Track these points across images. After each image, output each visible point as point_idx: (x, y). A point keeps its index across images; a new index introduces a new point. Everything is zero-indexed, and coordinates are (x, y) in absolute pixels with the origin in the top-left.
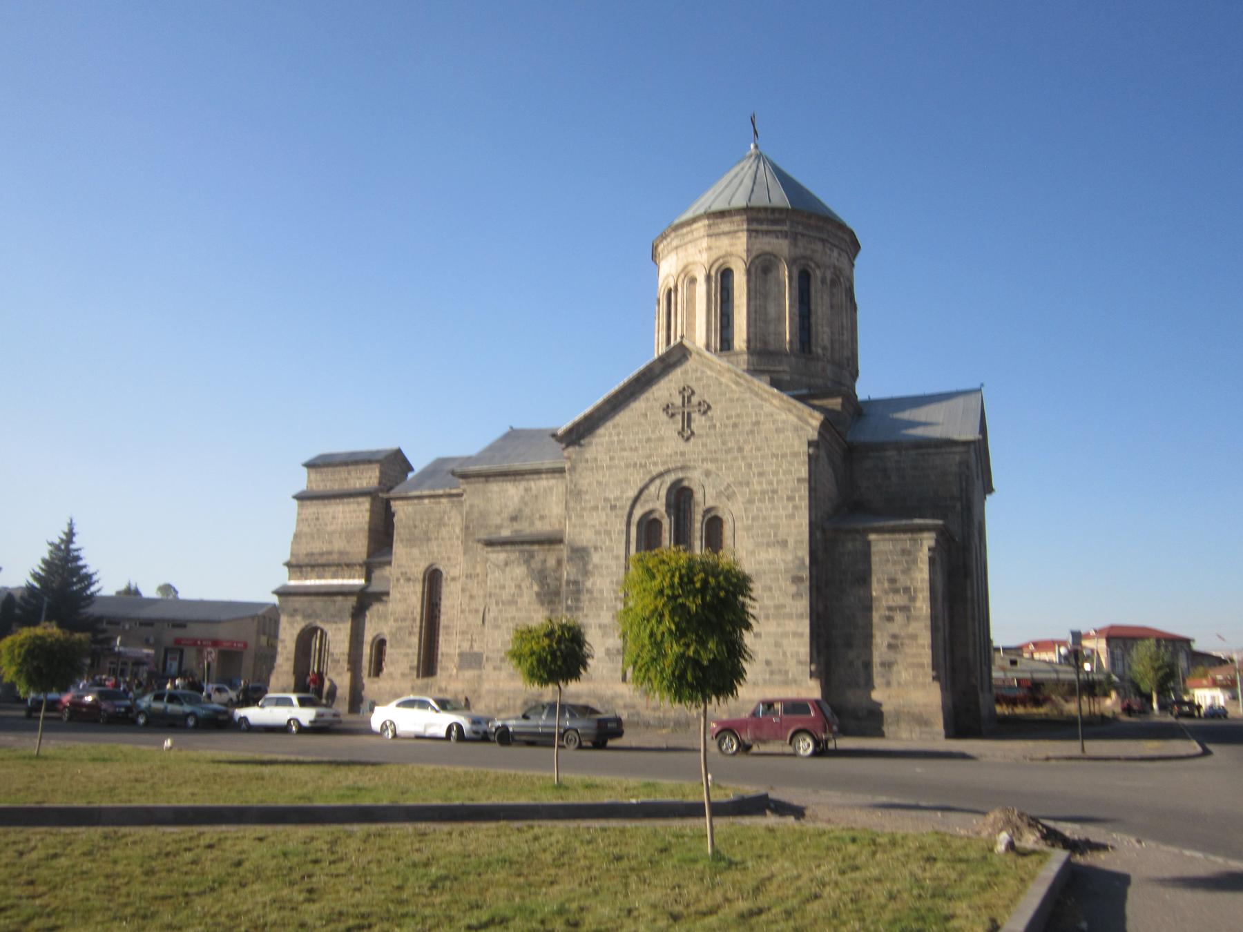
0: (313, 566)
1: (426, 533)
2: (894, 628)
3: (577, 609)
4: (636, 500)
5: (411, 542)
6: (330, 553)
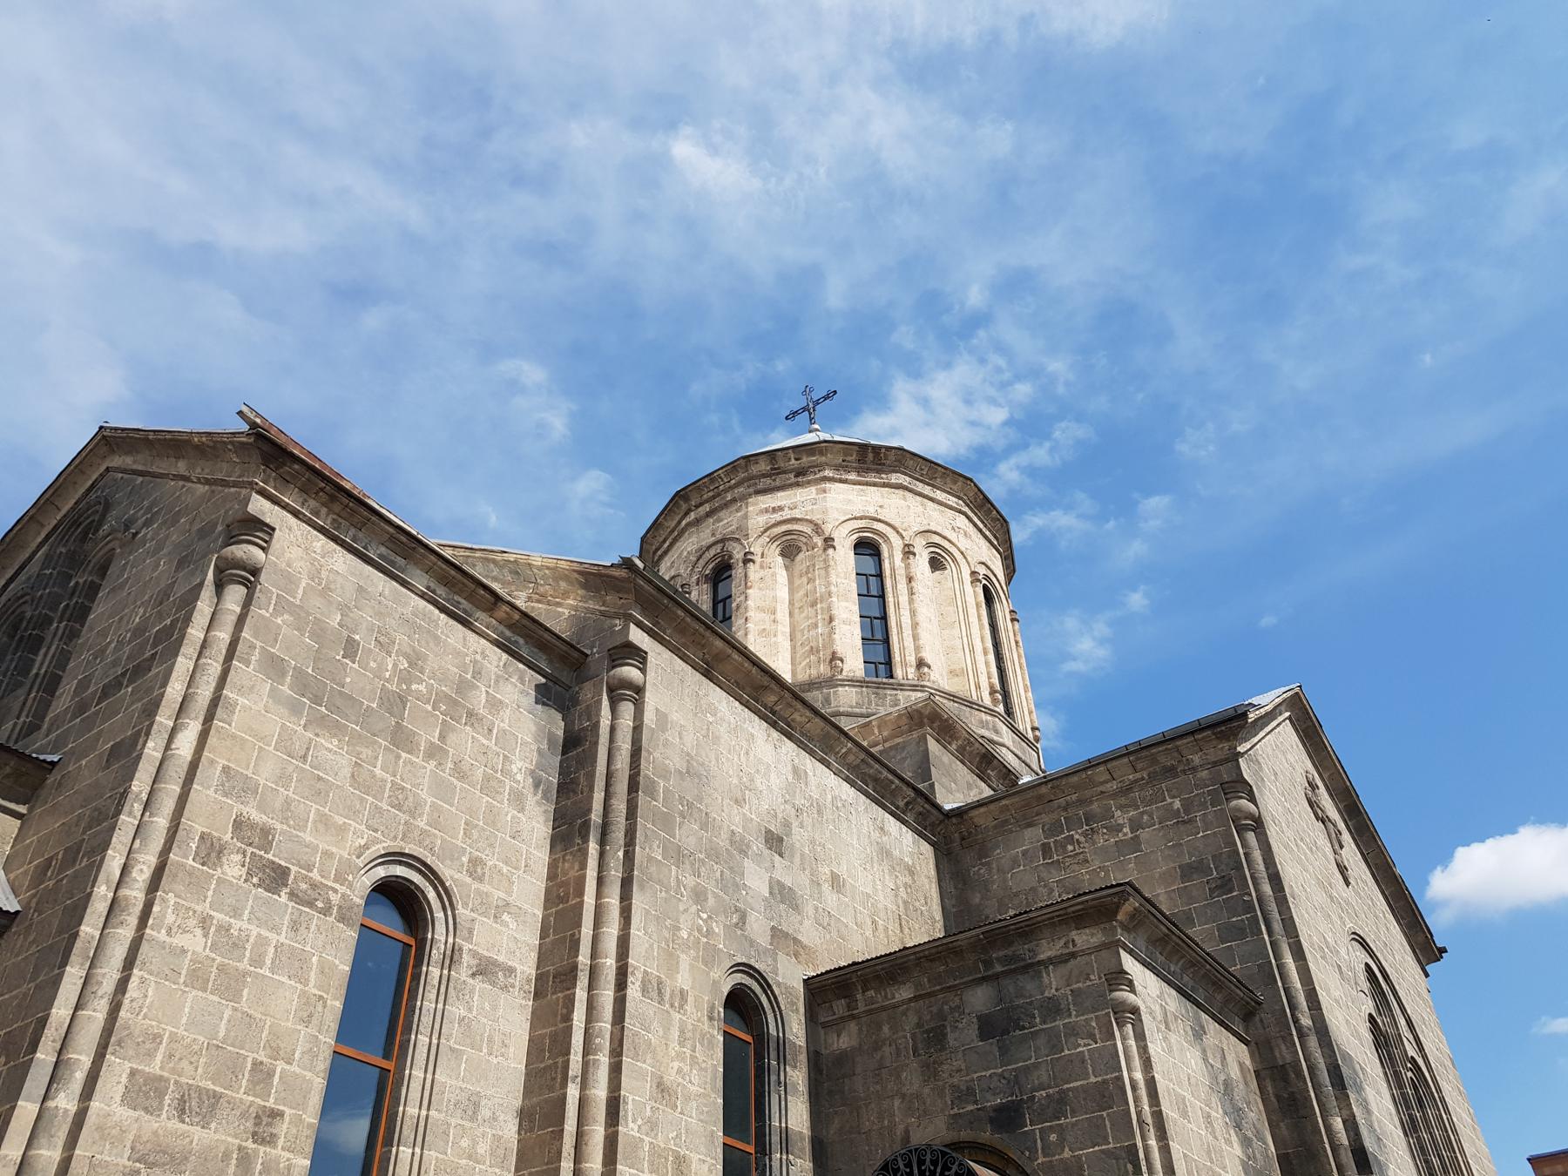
1: (395, 702)
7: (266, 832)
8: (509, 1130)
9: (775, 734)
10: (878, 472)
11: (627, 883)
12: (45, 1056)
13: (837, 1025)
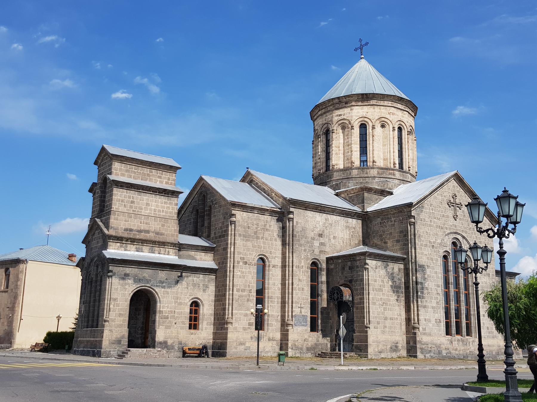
1: (256, 233)
3: (423, 297)
5: (247, 237)
6: (148, 232)
7: (244, 258)
8: (280, 286)
9: (321, 214)
10: (367, 101)
11: (293, 252)
12: (228, 287)
13: (331, 264)
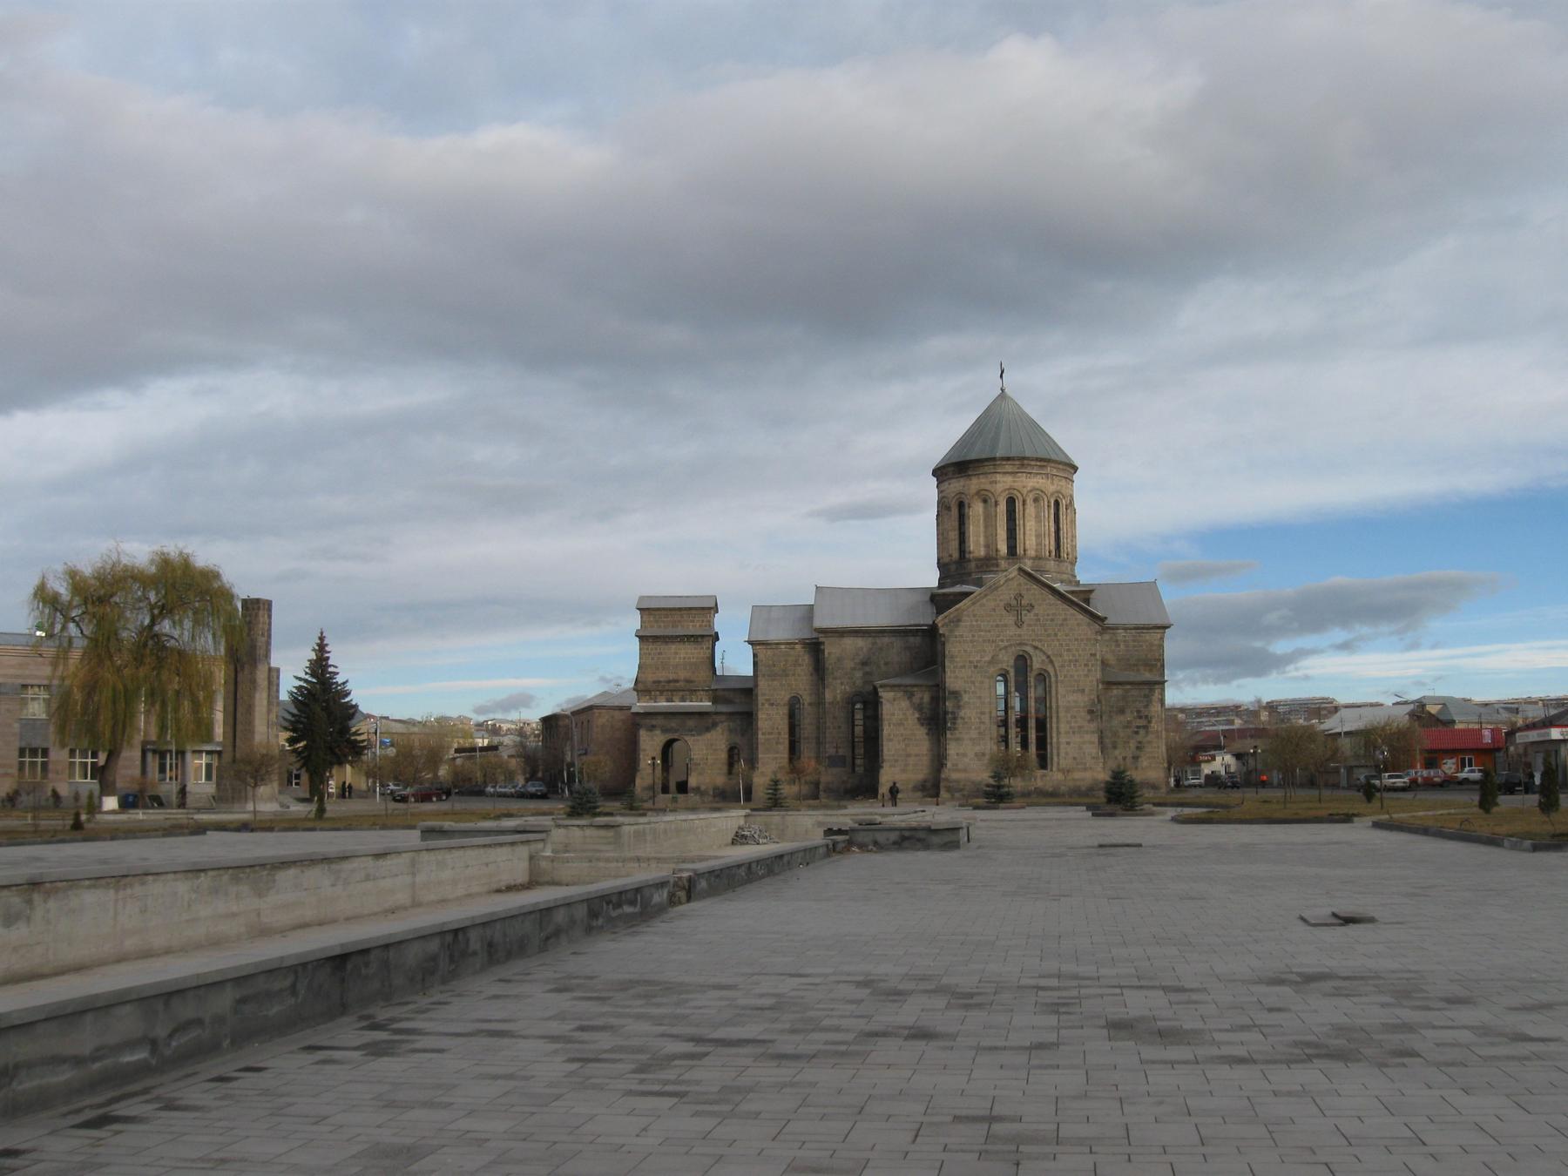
0: (662, 692)
2: (1139, 738)
4: (990, 662)
6: (676, 681)
